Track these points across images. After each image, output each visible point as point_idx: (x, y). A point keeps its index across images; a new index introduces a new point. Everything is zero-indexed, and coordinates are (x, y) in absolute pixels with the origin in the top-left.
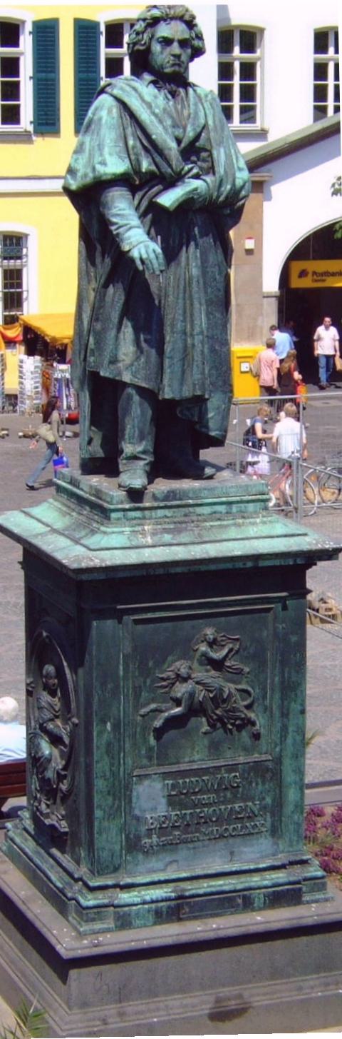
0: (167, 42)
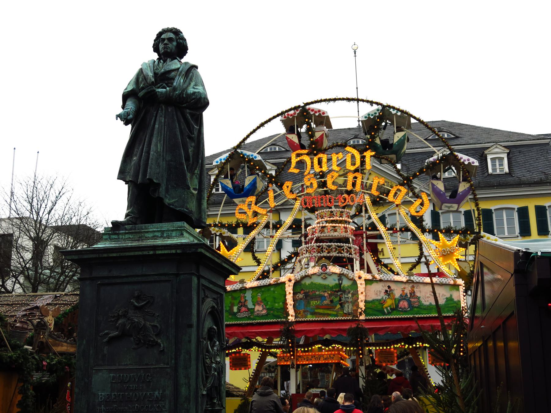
0: (164, 40)
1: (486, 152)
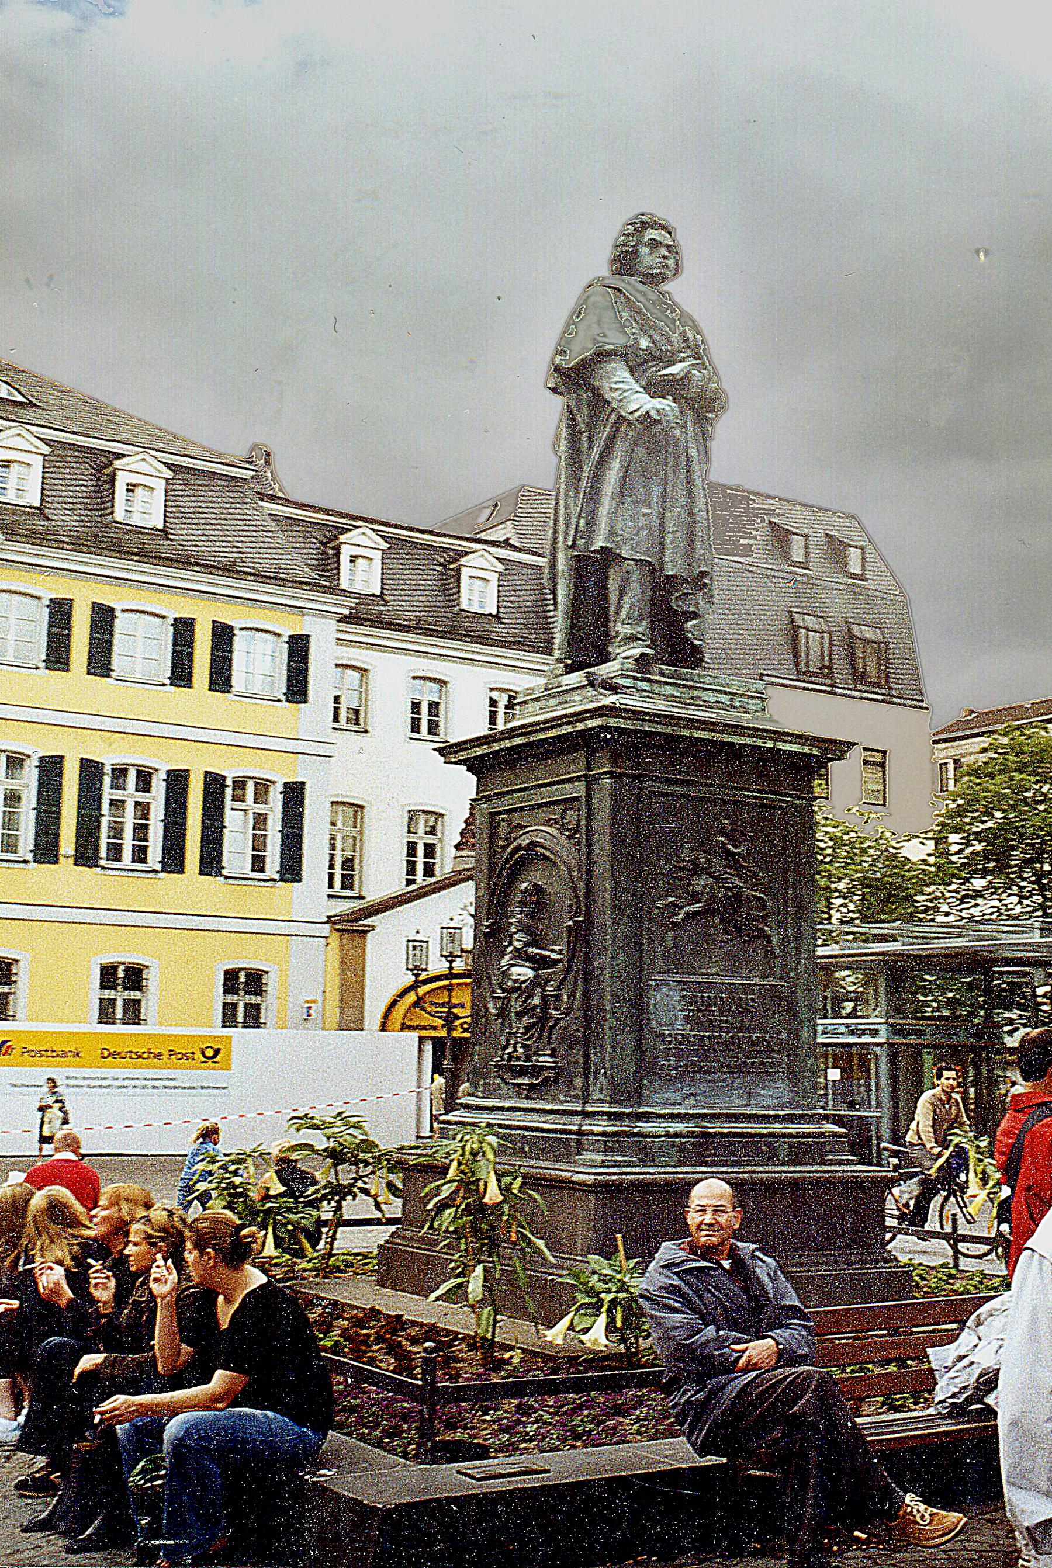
1: (118, 464)
